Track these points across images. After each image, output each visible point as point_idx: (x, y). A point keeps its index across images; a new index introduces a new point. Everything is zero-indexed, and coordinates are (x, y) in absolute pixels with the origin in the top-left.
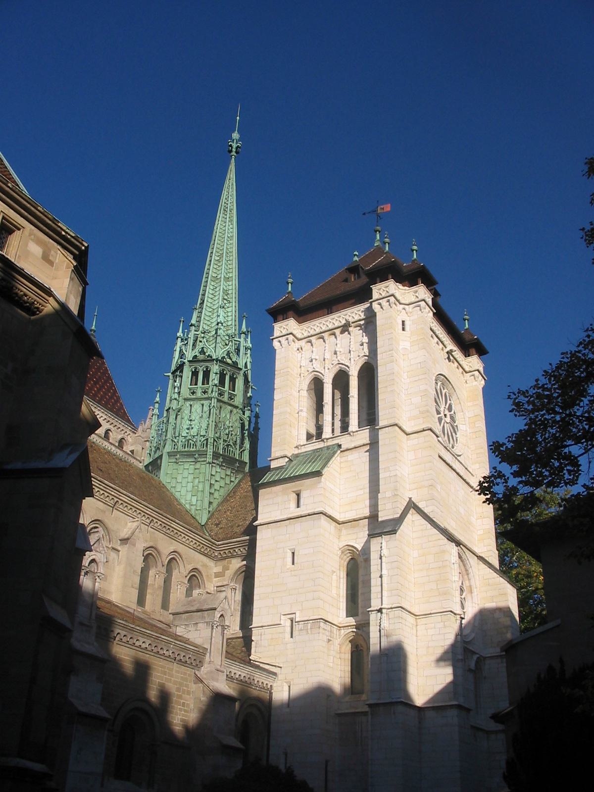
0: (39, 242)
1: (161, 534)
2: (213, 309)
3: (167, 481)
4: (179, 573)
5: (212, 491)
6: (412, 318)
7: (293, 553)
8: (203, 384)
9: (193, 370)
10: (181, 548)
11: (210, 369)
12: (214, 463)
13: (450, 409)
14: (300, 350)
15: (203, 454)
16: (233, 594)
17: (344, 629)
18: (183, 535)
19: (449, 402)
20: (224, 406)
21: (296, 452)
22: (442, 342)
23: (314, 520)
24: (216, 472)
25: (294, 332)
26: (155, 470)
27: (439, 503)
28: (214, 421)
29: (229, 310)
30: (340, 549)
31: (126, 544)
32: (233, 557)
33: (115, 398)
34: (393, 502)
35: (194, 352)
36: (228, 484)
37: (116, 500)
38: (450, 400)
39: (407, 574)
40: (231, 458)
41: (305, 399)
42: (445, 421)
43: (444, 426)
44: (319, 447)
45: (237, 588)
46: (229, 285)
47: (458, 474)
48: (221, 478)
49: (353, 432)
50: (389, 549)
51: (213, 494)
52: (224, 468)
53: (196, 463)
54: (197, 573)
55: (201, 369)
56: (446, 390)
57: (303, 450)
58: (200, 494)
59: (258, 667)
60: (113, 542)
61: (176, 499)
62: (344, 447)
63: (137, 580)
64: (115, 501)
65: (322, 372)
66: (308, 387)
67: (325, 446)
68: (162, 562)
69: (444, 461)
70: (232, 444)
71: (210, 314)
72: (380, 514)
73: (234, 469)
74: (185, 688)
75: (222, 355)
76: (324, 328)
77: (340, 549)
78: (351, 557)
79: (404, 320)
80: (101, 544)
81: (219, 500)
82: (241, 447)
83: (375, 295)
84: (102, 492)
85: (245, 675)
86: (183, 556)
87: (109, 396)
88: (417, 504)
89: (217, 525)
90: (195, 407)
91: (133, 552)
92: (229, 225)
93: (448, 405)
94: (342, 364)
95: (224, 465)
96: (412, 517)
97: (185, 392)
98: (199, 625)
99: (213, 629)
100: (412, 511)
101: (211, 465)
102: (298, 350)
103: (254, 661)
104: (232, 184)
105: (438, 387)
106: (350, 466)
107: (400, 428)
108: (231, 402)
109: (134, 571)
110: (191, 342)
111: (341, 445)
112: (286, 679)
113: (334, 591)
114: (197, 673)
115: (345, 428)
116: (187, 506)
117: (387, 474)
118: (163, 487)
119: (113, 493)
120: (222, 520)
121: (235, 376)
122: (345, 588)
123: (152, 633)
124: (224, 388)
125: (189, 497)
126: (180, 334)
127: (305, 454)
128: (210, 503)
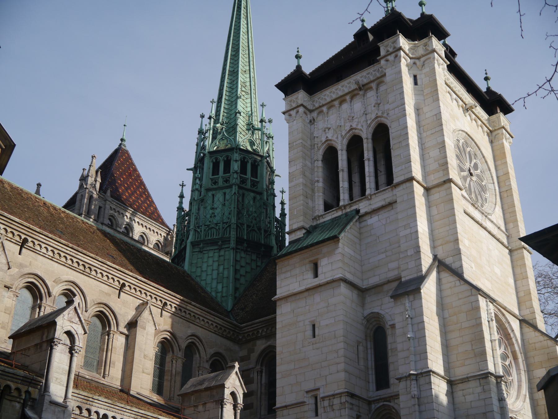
1: (176, 317)
2: (232, 102)
3: (192, 271)
6: (424, 71)
7: (314, 326)
8: (224, 173)
9: (214, 161)
10: (200, 332)
11: (231, 158)
12: (239, 249)
13: (476, 167)
14: (313, 122)
15: (226, 241)
16: (259, 377)
17: (374, 404)
18: (201, 318)
19: (474, 161)
20: (246, 193)
21: (315, 224)
23: (333, 288)
25: (305, 104)
26: (180, 262)
27: (468, 258)
28: (236, 207)
32: (258, 338)
34: (415, 260)
35: (214, 143)
36: (254, 269)
37: (122, 282)
39: (437, 336)
41: (321, 170)
43: (469, 185)
44: (337, 216)
47: (489, 232)
48: (247, 263)
49: (371, 195)
51: (239, 280)
52: (250, 253)
53: (220, 250)
55: (221, 159)
57: (322, 220)
61: (202, 288)
62: (362, 212)
64: (121, 283)
65: (336, 140)
67: (344, 213)
68: (179, 346)
70: (256, 229)
72: (403, 274)
76: (334, 96)
77: (365, 318)
78: (377, 326)
79: (415, 74)
82: (266, 231)
83: (383, 52)
86: (203, 341)
87: (141, 201)
88: (444, 261)
90: (217, 196)
94: (355, 129)
97: (206, 182)
98: (208, 405)
102: (310, 121)
105: (461, 144)
108: (254, 189)
109: (145, 355)
110: (210, 135)
116: (213, 294)
117: (408, 231)
122: (373, 359)
124: (246, 175)
125: (214, 284)
127: (323, 224)
128: (236, 289)
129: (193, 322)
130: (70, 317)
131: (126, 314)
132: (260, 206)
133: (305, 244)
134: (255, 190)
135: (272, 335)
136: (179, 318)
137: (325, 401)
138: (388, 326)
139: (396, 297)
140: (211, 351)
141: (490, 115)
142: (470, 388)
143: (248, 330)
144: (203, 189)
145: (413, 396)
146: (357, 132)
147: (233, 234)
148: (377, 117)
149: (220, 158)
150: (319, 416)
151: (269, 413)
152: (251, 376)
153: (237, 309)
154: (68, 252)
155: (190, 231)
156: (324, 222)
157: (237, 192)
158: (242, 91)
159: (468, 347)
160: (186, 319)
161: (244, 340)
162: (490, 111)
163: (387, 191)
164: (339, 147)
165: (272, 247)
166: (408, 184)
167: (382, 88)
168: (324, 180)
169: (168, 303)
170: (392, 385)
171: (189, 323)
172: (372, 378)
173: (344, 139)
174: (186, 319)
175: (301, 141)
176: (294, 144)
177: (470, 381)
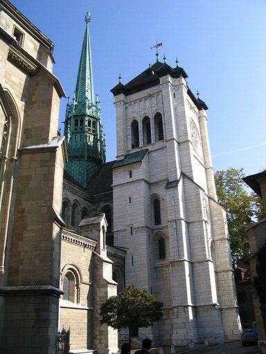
0: (32, 42)
10: (78, 198)
15: (83, 157)
83: (161, 82)
115: (149, 142)
138: (161, 199)
139: (167, 188)
140: (82, 207)
147: (86, 154)
159: (195, 209)
162: (200, 109)
164: (139, 121)
167: (160, 97)
172: (154, 220)
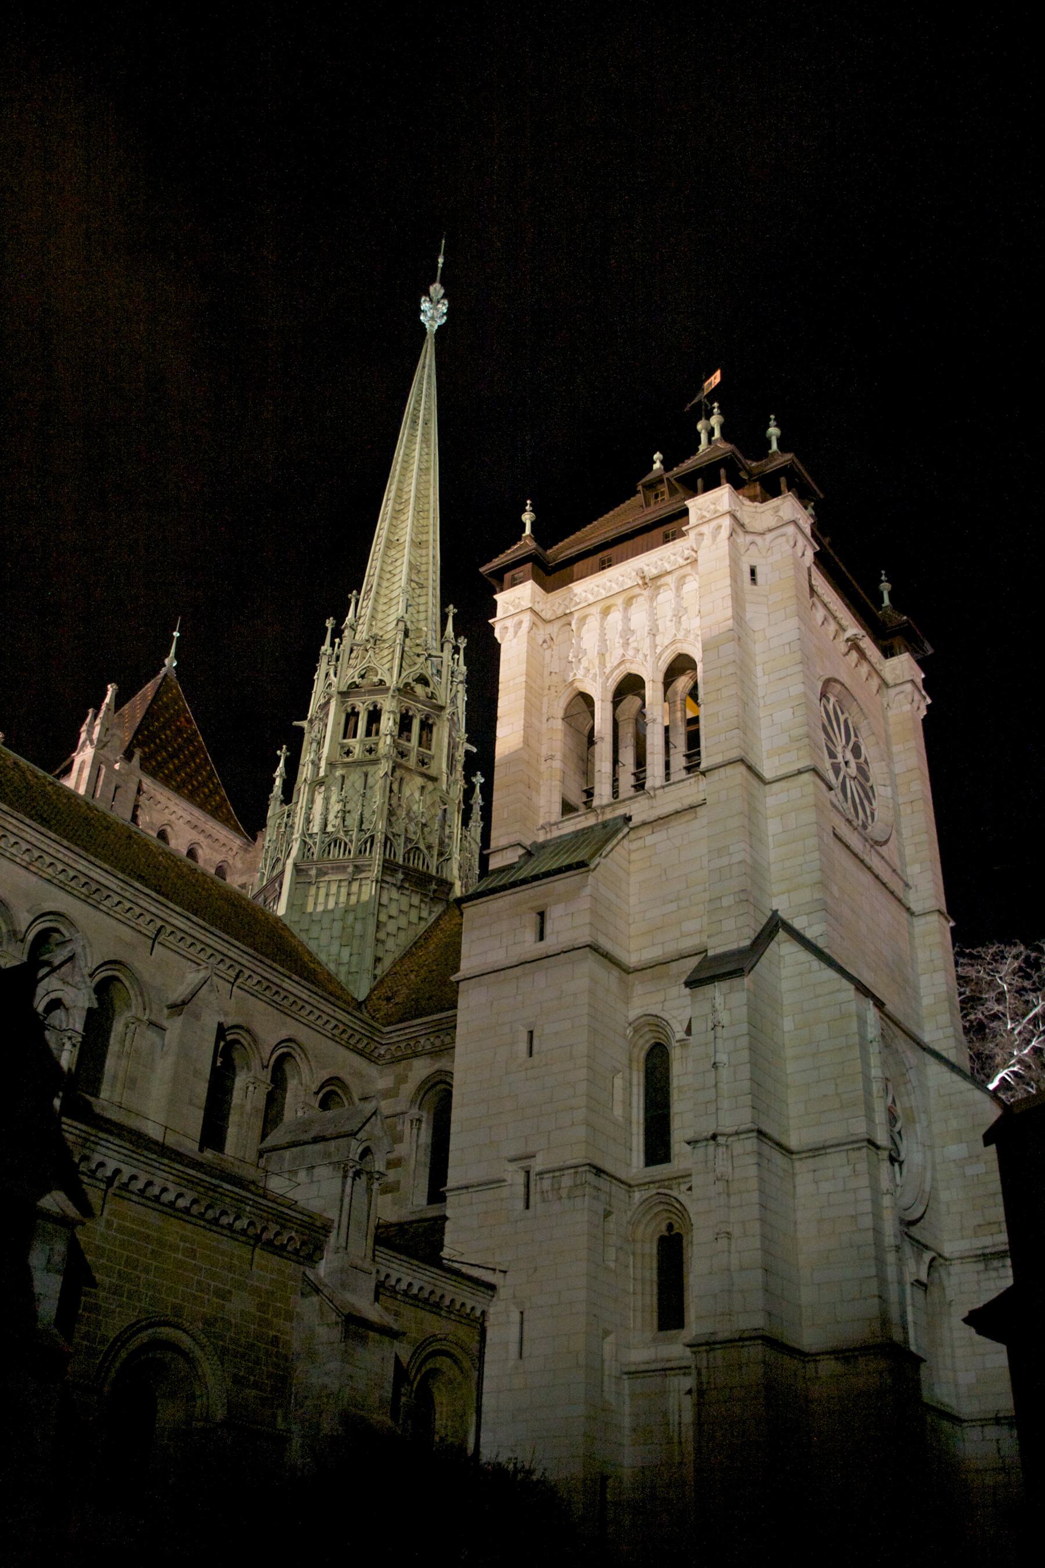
3: (293, 919)
4: (299, 1086)
5: (382, 935)
7: (531, 1032)
8: (368, 733)
10: (302, 1034)
12: (388, 883)
13: (856, 751)
16: (415, 1131)
17: (640, 1191)
20: (407, 777)
21: (541, 838)
22: (835, 618)
24: (391, 899)
25: (537, 608)
29: (422, 600)
30: (630, 1024)
31: (180, 1015)
32: (416, 1055)
33: (211, 786)
37: (160, 923)
38: (856, 736)
40: (425, 873)
41: (559, 736)
42: (847, 772)
45: (424, 1119)
46: (421, 556)
48: (401, 911)
49: (655, 789)
50: (730, 1009)
51: (383, 942)
54: (338, 1087)
56: (846, 715)
57: (556, 833)
58: (356, 943)
59: (457, 1273)
60: (151, 1011)
61: (310, 953)
63: (202, 1089)
64: (158, 926)
66: (565, 713)
67: (600, 821)
69: (848, 847)
71: (385, 608)
73: (426, 895)
74: (278, 1305)
75: (405, 681)
77: (630, 1024)
78: (653, 1041)
80: (76, 969)
81: (396, 955)
84: (128, 905)
85: (422, 1283)
88: (790, 922)
89: (388, 999)
91: (195, 1032)
92: (421, 448)
93: (851, 744)
95: (407, 885)
96: (783, 948)
98: (316, 1171)
99: (345, 1177)
100: (782, 935)
101: (379, 884)
103: (449, 1260)
104: (429, 376)
105: (831, 706)
106: (650, 856)
107: (750, 768)
108: (424, 769)
111: (629, 819)
112: (515, 1297)
113: (618, 1111)
114: (308, 1273)
115: (640, 786)
116: (332, 967)
118: (282, 929)
119: (153, 909)
120: (399, 990)
121: (430, 722)
123: (204, 1177)
125: (334, 949)
126: (326, 648)
127: (559, 841)
128: (378, 960)
129: (293, 1015)
130: (63, 974)
131: (163, 988)
132: (433, 804)
133: (523, 874)
134: (426, 772)
135: (447, 1050)
136: (265, 1005)
137: (543, 1181)
139: (693, 983)
140: (325, 1075)
141: (886, 657)
142: (829, 1168)
143: (399, 1039)
144: (323, 764)
145: (719, 1175)
146: (635, 669)
147: (377, 854)
148: (673, 642)
149: (361, 705)
150: (532, 1208)
151: (428, 1204)
152: (399, 1128)
153: (379, 999)
154: (60, 856)
155: (294, 842)
156: (560, 837)
157: (390, 773)
158: (412, 580)
160: (279, 1007)
161: (388, 1057)
163: (687, 783)
165: (452, 885)
166: (729, 770)
168: (564, 756)
169: (247, 973)
170: (676, 1158)
171: (282, 1015)
173: (608, 679)
174: (279, 1007)
175: (523, 678)
176: (511, 683)
177: (829, 1153)
